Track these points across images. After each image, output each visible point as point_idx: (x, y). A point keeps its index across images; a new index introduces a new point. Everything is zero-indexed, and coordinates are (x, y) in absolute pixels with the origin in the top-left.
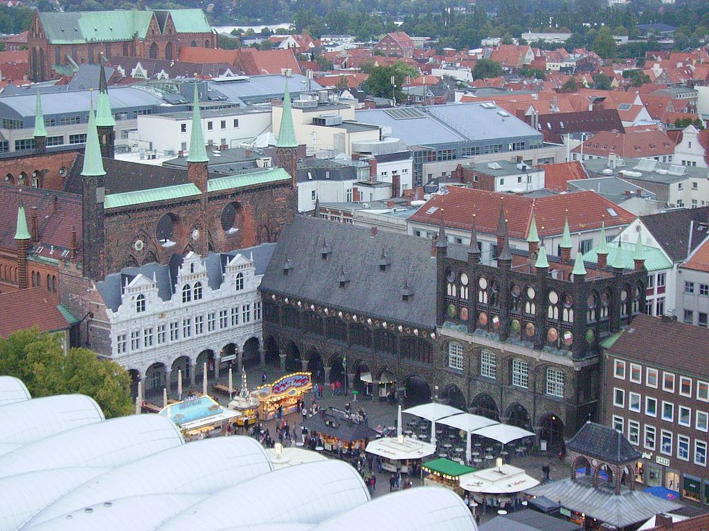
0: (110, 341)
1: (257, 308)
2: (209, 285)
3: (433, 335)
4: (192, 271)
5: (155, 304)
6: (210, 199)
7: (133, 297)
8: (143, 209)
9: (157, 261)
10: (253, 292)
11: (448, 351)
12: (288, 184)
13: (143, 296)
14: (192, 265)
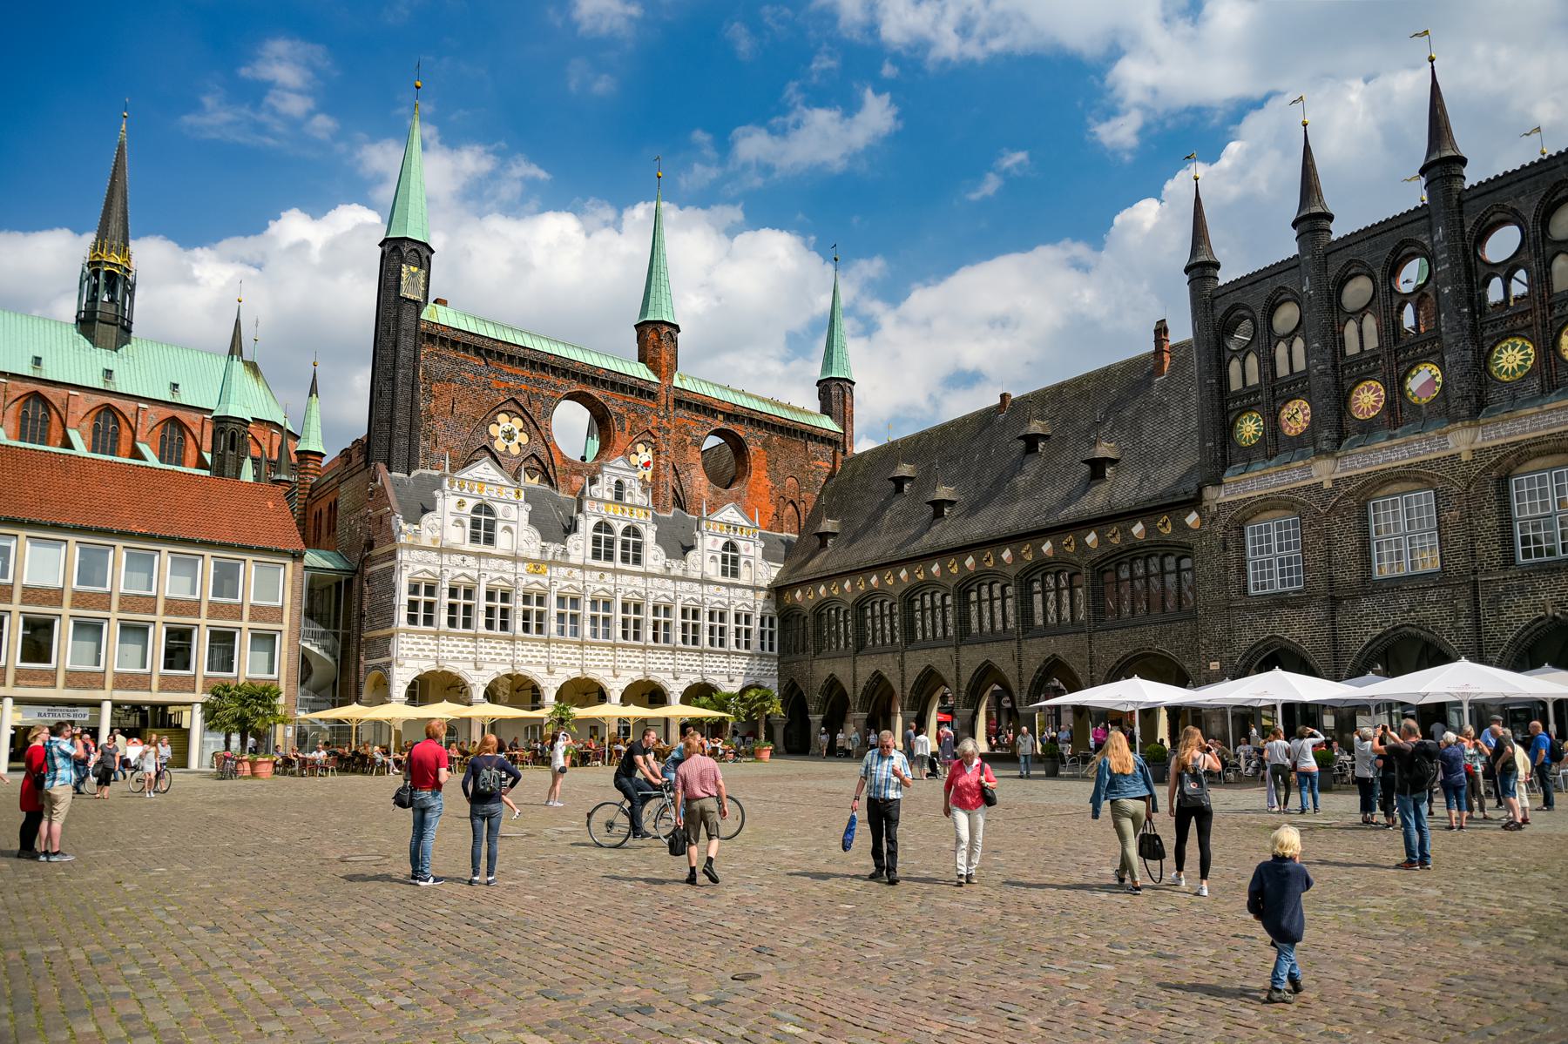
0: (391, 589)
1: (767, 627)
2: (659, 540)
3: (1192, 519)
4: (619, 496)
5: (517, 531)
6: (679, 403)
7: (461, 504)
8: (522, 361)
9: (551, 484)
10: (761, 589)
11: (1243, 548)
12: (837, 442)
13: (489, 511)
14: (619, 484)
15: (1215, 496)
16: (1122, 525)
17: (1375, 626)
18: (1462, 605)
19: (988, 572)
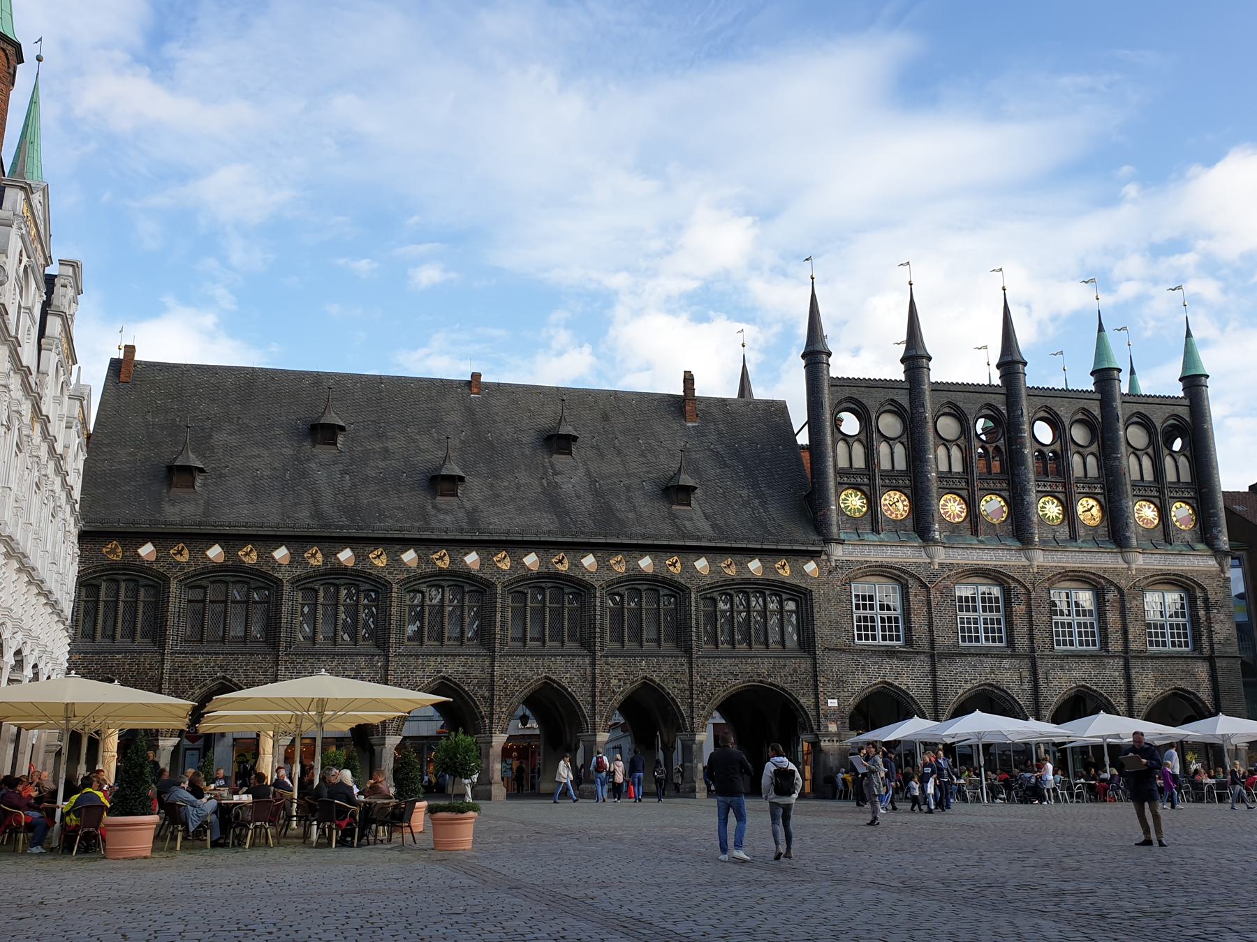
3: (811, 567)
15: (838, 552)
16: (739, 558)
17: (966, 682)
18: (1026, 673)
19: (558, 576)
